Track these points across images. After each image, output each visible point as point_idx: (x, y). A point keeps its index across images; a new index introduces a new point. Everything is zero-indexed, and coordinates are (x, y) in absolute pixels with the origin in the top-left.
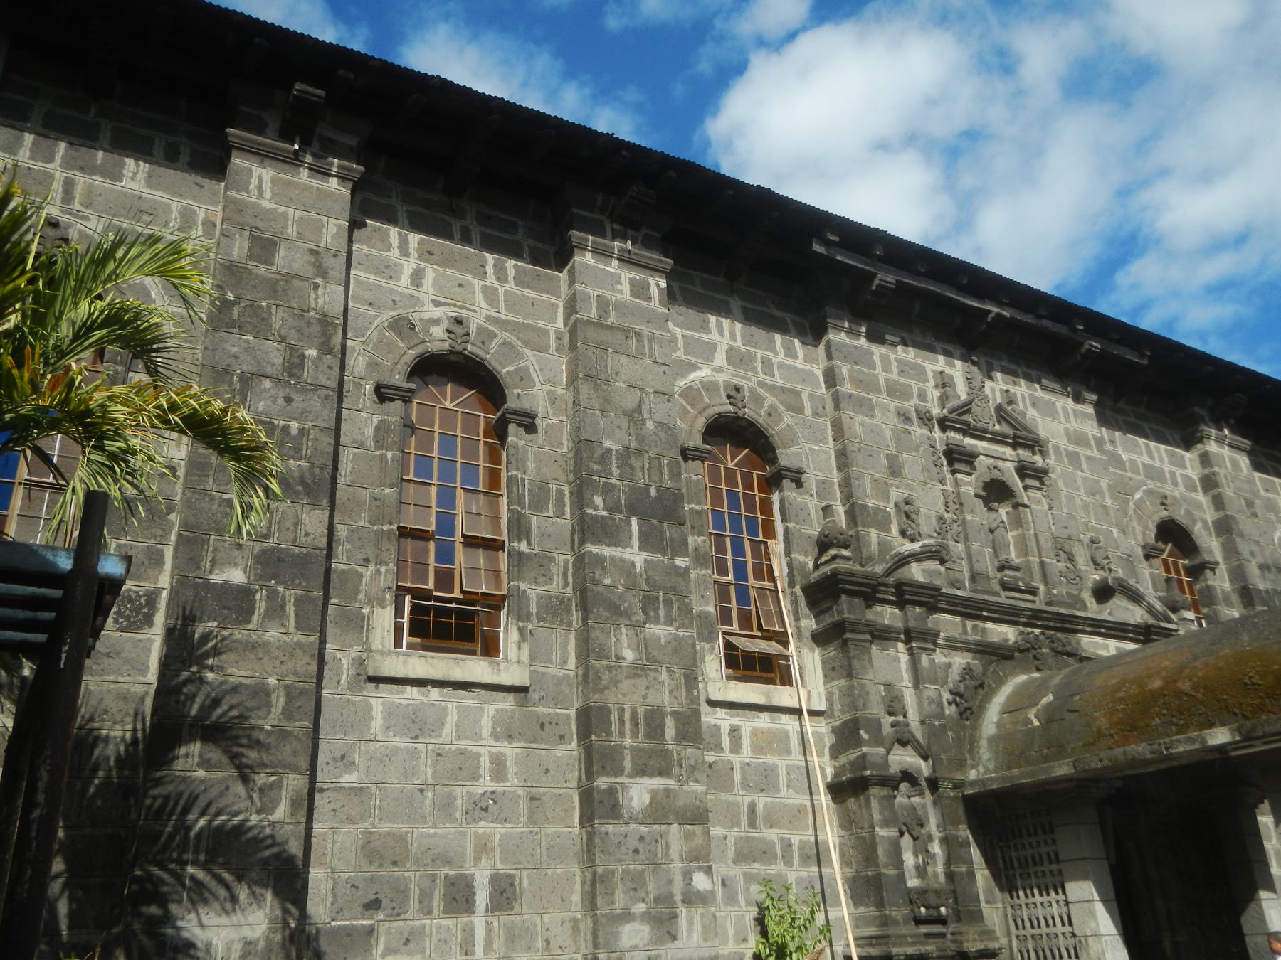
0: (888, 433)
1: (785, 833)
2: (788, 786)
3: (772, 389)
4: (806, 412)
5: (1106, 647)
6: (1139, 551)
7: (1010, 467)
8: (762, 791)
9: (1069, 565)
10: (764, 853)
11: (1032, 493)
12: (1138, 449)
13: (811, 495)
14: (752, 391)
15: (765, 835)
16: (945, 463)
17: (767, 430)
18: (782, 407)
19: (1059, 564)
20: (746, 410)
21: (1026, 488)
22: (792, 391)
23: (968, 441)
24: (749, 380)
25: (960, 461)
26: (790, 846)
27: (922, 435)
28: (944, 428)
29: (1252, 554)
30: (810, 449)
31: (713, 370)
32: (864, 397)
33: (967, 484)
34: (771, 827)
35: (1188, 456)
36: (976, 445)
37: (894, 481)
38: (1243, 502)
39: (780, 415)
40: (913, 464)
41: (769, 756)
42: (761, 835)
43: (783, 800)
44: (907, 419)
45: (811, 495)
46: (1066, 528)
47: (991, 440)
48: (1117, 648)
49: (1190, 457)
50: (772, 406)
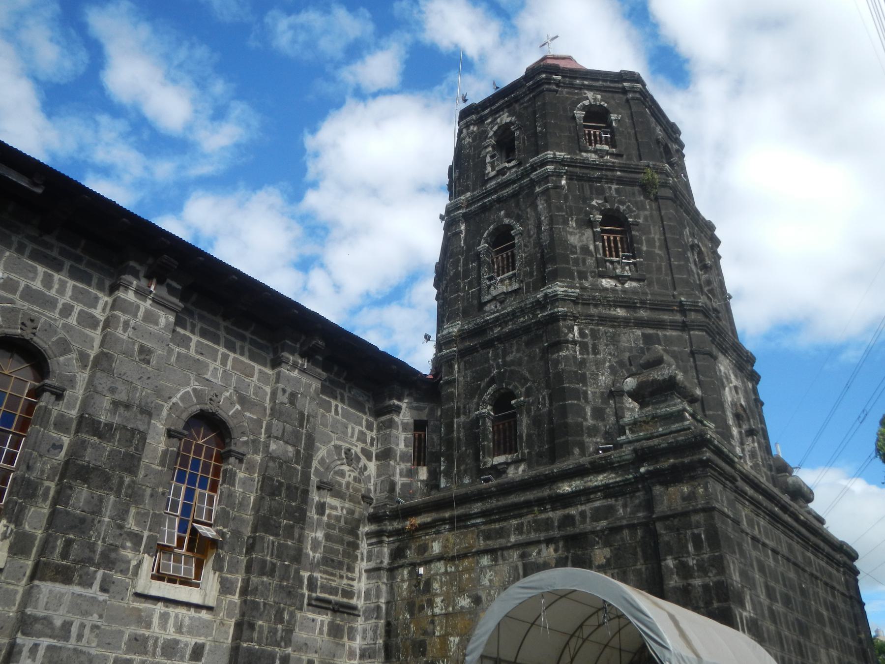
12: (31, 275)
29: (112, 390)
35: (106, 299)
49: (105, 299)
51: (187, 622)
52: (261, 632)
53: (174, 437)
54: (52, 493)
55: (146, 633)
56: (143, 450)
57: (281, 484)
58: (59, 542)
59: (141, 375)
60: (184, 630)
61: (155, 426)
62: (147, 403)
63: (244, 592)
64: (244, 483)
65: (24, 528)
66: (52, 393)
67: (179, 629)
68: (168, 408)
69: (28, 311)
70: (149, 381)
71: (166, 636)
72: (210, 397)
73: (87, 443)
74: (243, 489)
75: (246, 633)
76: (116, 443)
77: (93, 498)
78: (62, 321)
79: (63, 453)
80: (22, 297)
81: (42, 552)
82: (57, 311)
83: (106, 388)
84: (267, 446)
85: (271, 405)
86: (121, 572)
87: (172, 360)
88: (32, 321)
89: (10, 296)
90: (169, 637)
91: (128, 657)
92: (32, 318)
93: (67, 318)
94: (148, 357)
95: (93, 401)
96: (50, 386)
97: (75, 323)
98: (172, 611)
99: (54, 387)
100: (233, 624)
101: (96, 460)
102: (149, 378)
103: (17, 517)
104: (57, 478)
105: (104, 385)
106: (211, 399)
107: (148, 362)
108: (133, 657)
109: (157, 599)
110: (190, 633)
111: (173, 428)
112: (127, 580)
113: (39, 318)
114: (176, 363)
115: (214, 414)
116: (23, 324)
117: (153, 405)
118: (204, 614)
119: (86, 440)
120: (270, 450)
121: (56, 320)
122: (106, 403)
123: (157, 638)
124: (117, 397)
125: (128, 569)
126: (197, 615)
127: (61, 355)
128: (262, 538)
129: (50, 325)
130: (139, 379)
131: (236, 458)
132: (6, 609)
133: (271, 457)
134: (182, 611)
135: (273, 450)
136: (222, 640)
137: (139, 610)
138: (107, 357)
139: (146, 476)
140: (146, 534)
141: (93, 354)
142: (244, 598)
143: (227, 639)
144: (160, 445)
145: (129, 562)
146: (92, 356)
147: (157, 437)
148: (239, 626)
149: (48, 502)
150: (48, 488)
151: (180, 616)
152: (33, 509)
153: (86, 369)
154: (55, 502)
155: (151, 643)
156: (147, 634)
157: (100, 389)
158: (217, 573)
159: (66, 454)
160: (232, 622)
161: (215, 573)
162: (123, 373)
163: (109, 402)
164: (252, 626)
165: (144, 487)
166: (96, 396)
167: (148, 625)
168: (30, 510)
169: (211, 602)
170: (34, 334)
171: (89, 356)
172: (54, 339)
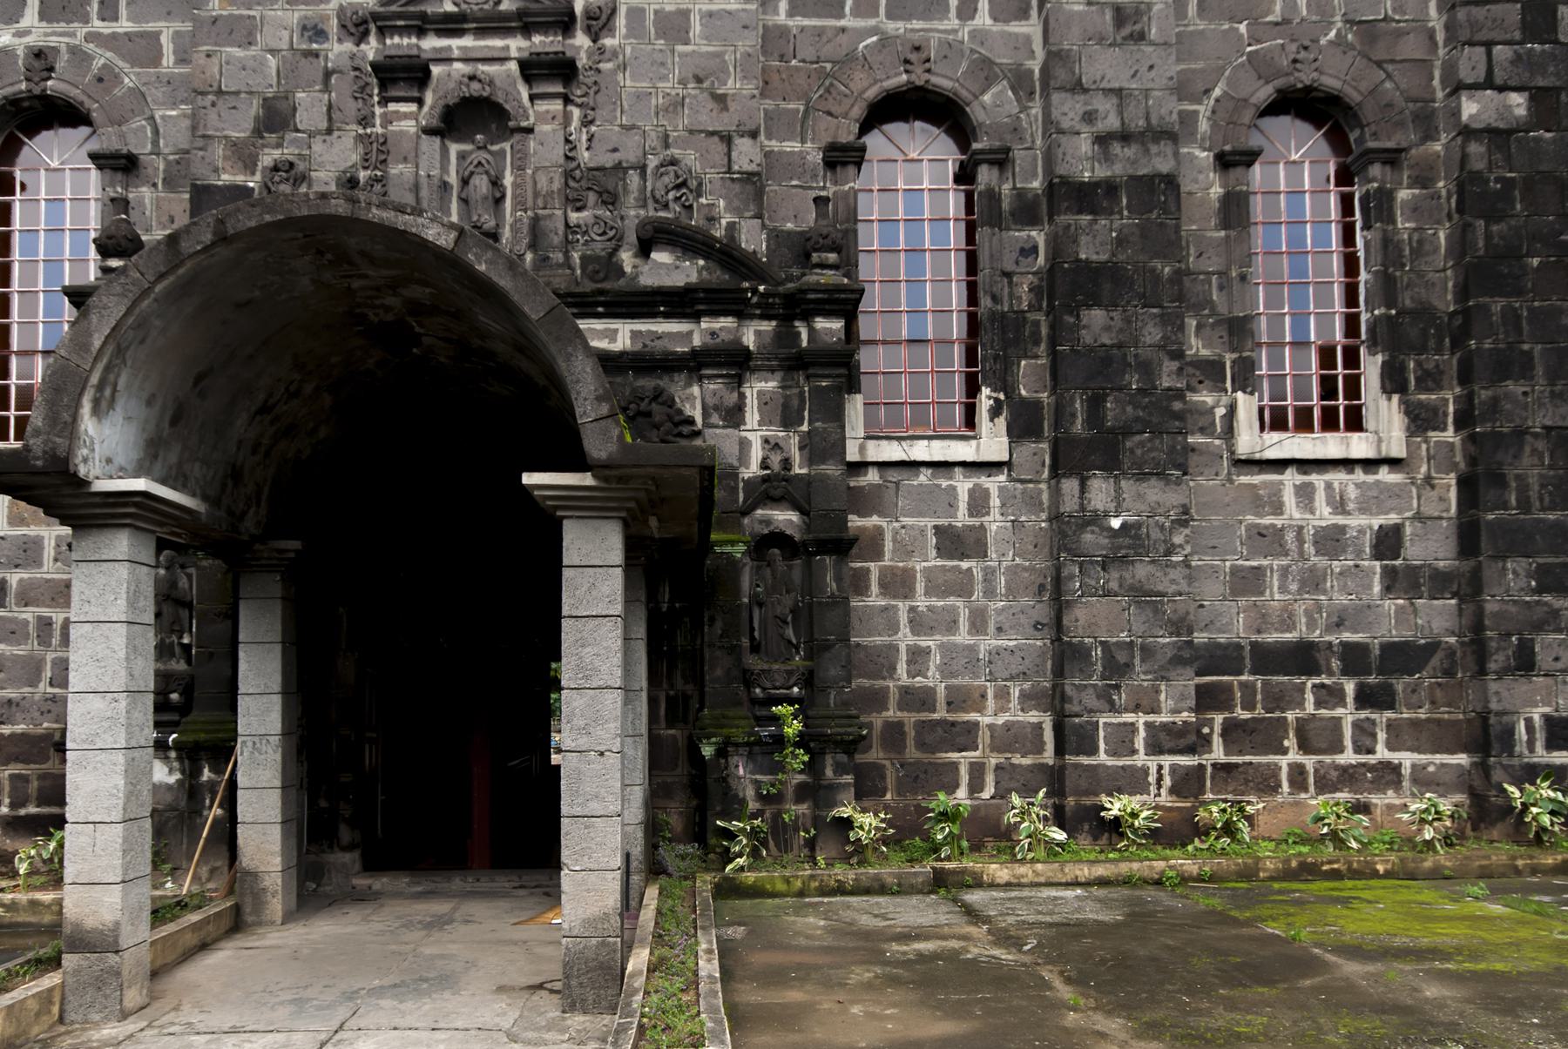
0: (272, 62)
1: (45, 612)
2: (56, 560)
3: (110, 41)
4: (164, 62)
5: (612, 335)
6: (817, 157)
7: (513, 66)
8: (16, 566)
9: (604, 213)
10: (13, 633)
11: (543, 106)
13: (155, 185)
14: (74, 50)
15: (16, 615)
16: (376, 91)
17: (82, 103)
18: (121, 64)
19: (585, 214)
20: (49, 83)
21: (532, 98)
22: (142, 35)
23: (431, 43)
24: (73, 35)
25: (394, 81)
26: (50, 624)
27: (340, 54)
28: (382, 32)
29: (1089, 117)
30: (163, 117)
31: (14, 35)
32: (241, 16)
33: (406, 116)
34: (26, 605)
36: (449, 48)
37: (271, 138)
38: (1109, 16)
39: (117, 76)
40: (309, 108)
41: (32, 527)
42: (10, 615)
43: (45, 576)
44: (319, 34)
45: (155, 185)
46: (615, 150)
47: (481, 32)
48: (635, 335)
50: (105, 65)
51: (1352, 493)
52: (1523, 489)
53: (1235, 164)
54: (1044, 331)
55: (1276, 522)
56: (1179, 209)
57: (1508, 184)
58: (1078, 405)
59: (1135, 68)
60: (1351, 506)
61: (1192, 157)
62: (1162, 118)
63: (1462, 422)
64: (1414, 209)
65: (1020, 394)
66: (991, 163)
67: (1340, 506)
68: (1208, 114)
69: (909, 36)
70: (1153, 73)
71: (1317, 523)
72: (1292, 57)
73: (1073, 228)
74: (1416, 221)
75: (1488, 494)
76: (1125, 213)
77: (1112, 319)
78: (966, 30)
79: (1041, 260)
80: (890, 16)
81: (1057, 425)
82: (953, 12)
83: (1077, 119)
84: (1456, 113)
85: (1444, 18)
86: (1202, 430)
87: (1190, 14)
88: (917, 49)
89: (872, 22)
90: (1324, 524)
91: (1255, 563)
92: (917, 44)
93: (973, 18)
94: (1137, 27)
95: (1060, 151)
96: (982, 152)
97: (989, 21)
98: (1318, 479)
99: (991, 151)
100: (1453, 482)
101: (1097, 253)
102: (1151, 67)
103: (1005, 381)
104: (1045, 304)
105: (1071, 115)
106: (1295, 61)
107: (1141, 37)
108: (1265, 563)
109: (1281, 465)
110: (1363, 510)
111: (1228, 148)
112: (1217, 442)
113: (928, 40)
114: (1199, 15)
115: (1308, 89)
116: (907, 61)
117: (1175, 116)
118: (1385, 475)
119: (1070, 225)
120: (1465, 117)
121: (955, 31)
122: (1084, 145)
123: (1301, 528)
124: (1101, 127)
125: (1213, 423)
126: (1371, 478)
127: (983, 92)
128: (1485, 309)
129: (949, 44)
130: (1134, 76)
131: (1384, 163)
132: (1033, 518)
133: (1467, 133)
134: (1338, 477)
135: (1471, 116)
136: (1436, 514)
137: (1254, 486)
138: (1061, 59)
139: (1201, 255)
140: (1229, 358)
141: (1035, 66)
142: (1465, 433)
143: (1448, 510)
144: (1212, 191)
145: (1211, 411)
146: (1037, 71)
147: (1201, 177)
148: (1465, 484)
149: (1043, 346)
150: (1037, 324)
151: (1336, 485)
152: (1023, 363)
153: (1034, 99)
154: (1053, 342)
155: (1290, 537)
156: (1279, 522)
157: (1065, 124)
158: (1395, 398)
159: (1046, 260)
160: (1451, 479)
161: (1389, 399)
162: (1098, 78)
163: (1089, 141)
164: (1500, 481)
165: (1202, 277)
166: (1063, 139)
167: (1278, 509)
168: (1019, 365)
169: (1397, 449)
170: (928, 71)
171: (1032, 72)
172: (964, 66)
